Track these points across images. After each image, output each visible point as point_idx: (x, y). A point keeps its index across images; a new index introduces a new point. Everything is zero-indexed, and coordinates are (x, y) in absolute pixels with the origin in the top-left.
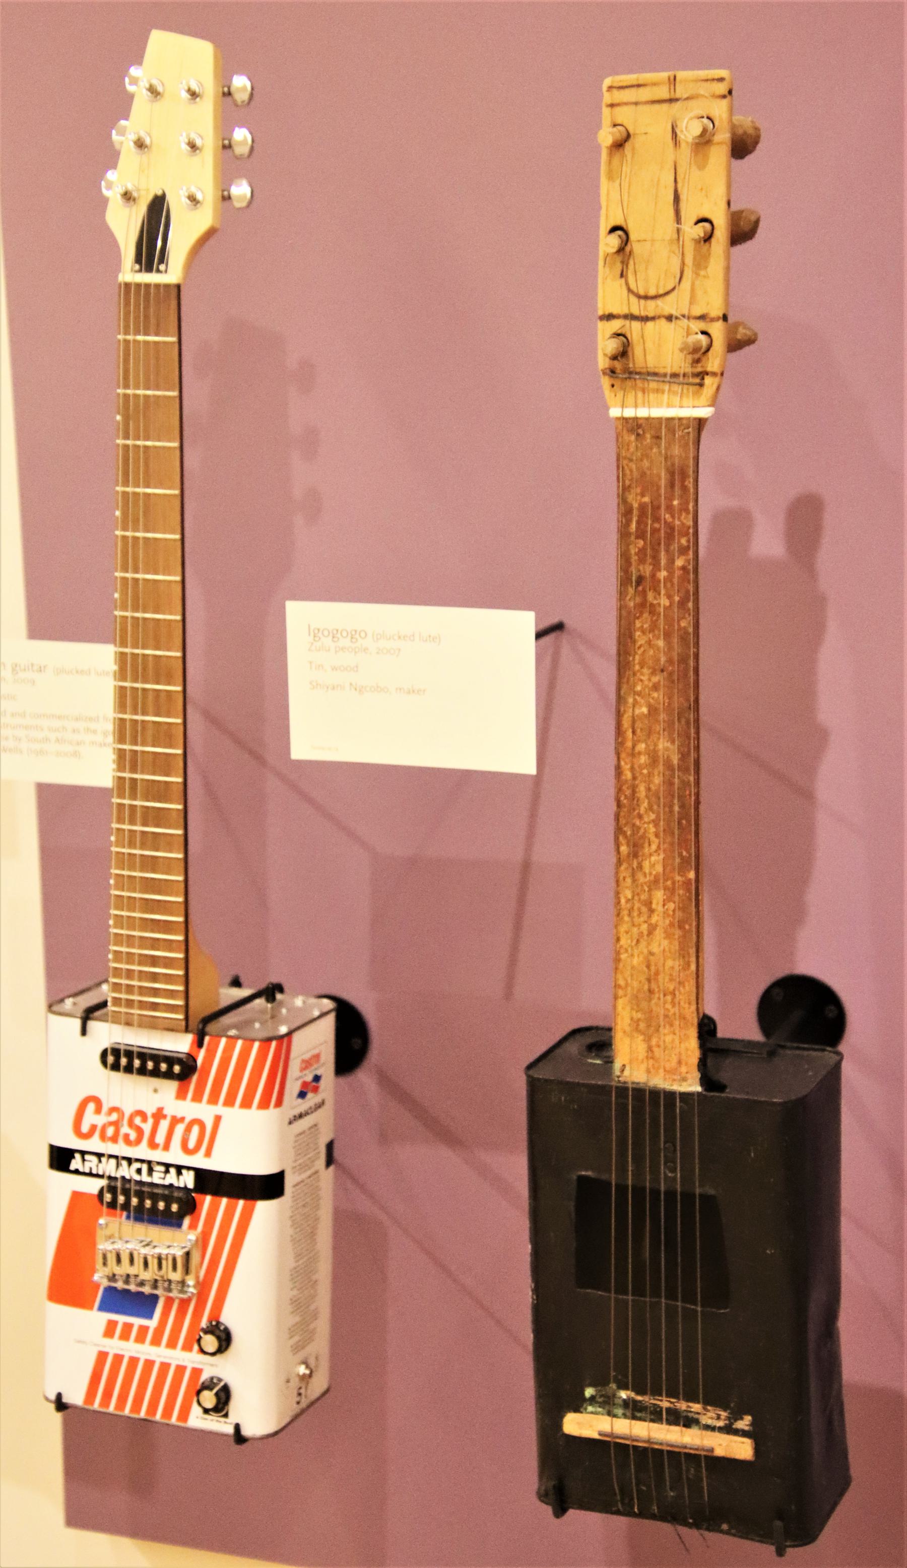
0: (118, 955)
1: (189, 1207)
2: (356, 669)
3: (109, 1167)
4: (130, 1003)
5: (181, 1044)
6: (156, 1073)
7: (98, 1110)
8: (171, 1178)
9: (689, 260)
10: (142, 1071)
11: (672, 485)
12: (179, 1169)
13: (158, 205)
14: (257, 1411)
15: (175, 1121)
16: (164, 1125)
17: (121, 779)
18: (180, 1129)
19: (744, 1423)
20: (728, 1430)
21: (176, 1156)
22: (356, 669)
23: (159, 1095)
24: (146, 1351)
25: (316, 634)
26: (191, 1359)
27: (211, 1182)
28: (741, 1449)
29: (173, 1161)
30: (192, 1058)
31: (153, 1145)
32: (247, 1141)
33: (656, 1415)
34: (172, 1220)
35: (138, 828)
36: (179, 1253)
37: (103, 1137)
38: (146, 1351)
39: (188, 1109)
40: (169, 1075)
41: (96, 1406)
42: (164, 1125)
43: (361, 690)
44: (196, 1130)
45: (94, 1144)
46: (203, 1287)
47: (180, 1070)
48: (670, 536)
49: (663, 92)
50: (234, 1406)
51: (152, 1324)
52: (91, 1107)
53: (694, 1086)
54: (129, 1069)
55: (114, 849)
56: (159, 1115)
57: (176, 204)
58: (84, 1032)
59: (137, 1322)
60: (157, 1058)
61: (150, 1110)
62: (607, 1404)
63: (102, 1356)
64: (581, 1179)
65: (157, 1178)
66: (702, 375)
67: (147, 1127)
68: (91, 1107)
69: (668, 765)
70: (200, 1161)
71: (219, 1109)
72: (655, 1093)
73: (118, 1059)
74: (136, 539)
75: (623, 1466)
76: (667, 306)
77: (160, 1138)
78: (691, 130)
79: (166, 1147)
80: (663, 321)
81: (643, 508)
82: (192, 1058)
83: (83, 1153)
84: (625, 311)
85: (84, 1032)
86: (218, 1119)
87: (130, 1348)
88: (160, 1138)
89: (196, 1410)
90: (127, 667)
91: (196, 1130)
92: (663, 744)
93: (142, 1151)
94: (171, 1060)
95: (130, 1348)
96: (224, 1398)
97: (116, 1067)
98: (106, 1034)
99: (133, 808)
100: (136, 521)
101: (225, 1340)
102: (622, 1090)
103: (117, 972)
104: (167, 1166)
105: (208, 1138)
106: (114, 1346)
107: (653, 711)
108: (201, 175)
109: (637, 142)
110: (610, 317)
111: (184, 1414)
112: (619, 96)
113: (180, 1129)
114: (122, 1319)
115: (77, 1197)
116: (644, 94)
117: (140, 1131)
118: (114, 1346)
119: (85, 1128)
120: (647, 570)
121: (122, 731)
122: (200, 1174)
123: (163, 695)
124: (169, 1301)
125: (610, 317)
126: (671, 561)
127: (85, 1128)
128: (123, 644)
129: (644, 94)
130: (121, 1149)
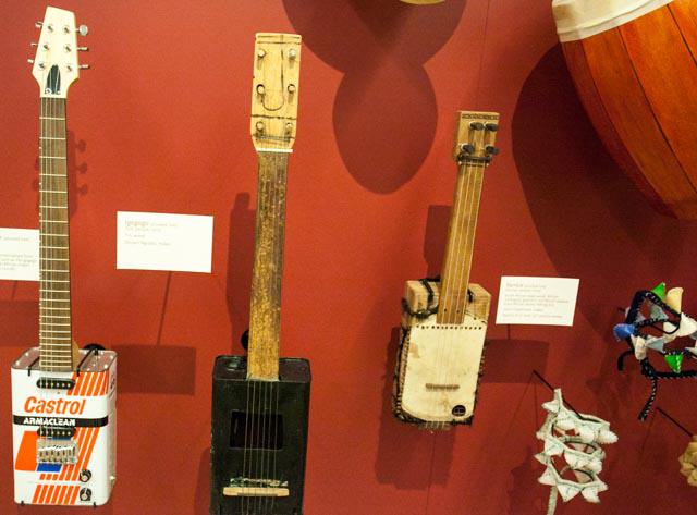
0: (44, 334)
1: (74, 433)
2: (143, 236)
3: (40, 421)
4: (49, 364)
5: (69, 376)
6: (60, 387)
7: (35, 401)
8: (66, 423)
9: (287, 98)
10: (55, 387)
11: (278, 175)
12: (69, 420)
13: (55, 69)
14: (100, 497)
15: (67, 403)
16: (62, 405)
17: (44, 273)
18: (69, 406)
19: (285, 484)
20: (280, 487)
21: (67, 414)
22: (143, 236)
23: (63, 395)
24: (58, 483)
25: (129, 223)
26: (77, 483)
27: (82, 423)
28: (284, 492)
29: (68, 416)
30: (73, 380)
31: (58, 412)
32: (97, 406)
33: (258, 485)
34: (67, 437)
35: (52, 291)
36: (72, 449)
37: (38, 411)
38: (58, 483)
39: (72, 398)
40: (66, 388)
41: (38, 503)
42: (62, 405)
43: (145, 244)
44: (75, 405)
45: (34, 414)
46: (80, 458)
47: (69, 386)
48: (277, 193)
49: (278, 40)
50: (92, 498)
51: (60, 473)
52: (32, 401)
53: (277, 380)
54: (49, 387)
55: (41, 221)
56: (60, 401)
57: (62, 70)
58: (29, 375)
59: (53, 473)
60: (60, 382)
61: (56, 400)
62: (239, 483)
63: (39, 487)
64: (234, 413)
65: (60, 423)
66: (289, 138)
67: (55, 406)
68: (32, 401)
69: (274, 273)
70: (77, 416)
71: (85, 397)
72: (263, 383)
73: (42, 384)
74: (48, 194)
75: (245, 503)
76: (279, 113)
77: (61, 409)
78: (287, 55)
79: (64, 412)
80: (276, 119)
81: (267, 183)
82: (73, 380)
83: (29, 418)
84: (262, 114)
85: (29, 375)
86: (84, 401)
87: (51, 482)
88: (61, 409)
89: (78, 498)
90: (43, 239)
91: (75, 405)
92: (271, 265)
93: (54, 414)
94: (66, 383)
95: (51, 482)
96: (89, 493)
97: (44, 386)
98: (37, 375)
99: (49, 283)
100: (48, 187)
101: (88, 474)
102: (252, 382)
103: (44, 341)
104: (64, 419)
105: (81, 407)
106: (44, 482)
107: (268, 254)
108: (72, 59)
109: (269, 56)
110: (257, 116)
111: (73, 501)
112: (262, 40)
113: (69, 406)
114: (47, 473)
115: (27, 434)
116: (271, 40)
117: (53, 408)
118: (44, 482)
119: (29, 408)
120: (268, 205)
121: (43, 253)
122: (77, 420)
123: (59, 196)
124: (66, 466)
125: (257, 116)
126: (277, 201)
127: (29, 408)
128: (44, 232)
129: (271, 40)
130: (45, 415)
